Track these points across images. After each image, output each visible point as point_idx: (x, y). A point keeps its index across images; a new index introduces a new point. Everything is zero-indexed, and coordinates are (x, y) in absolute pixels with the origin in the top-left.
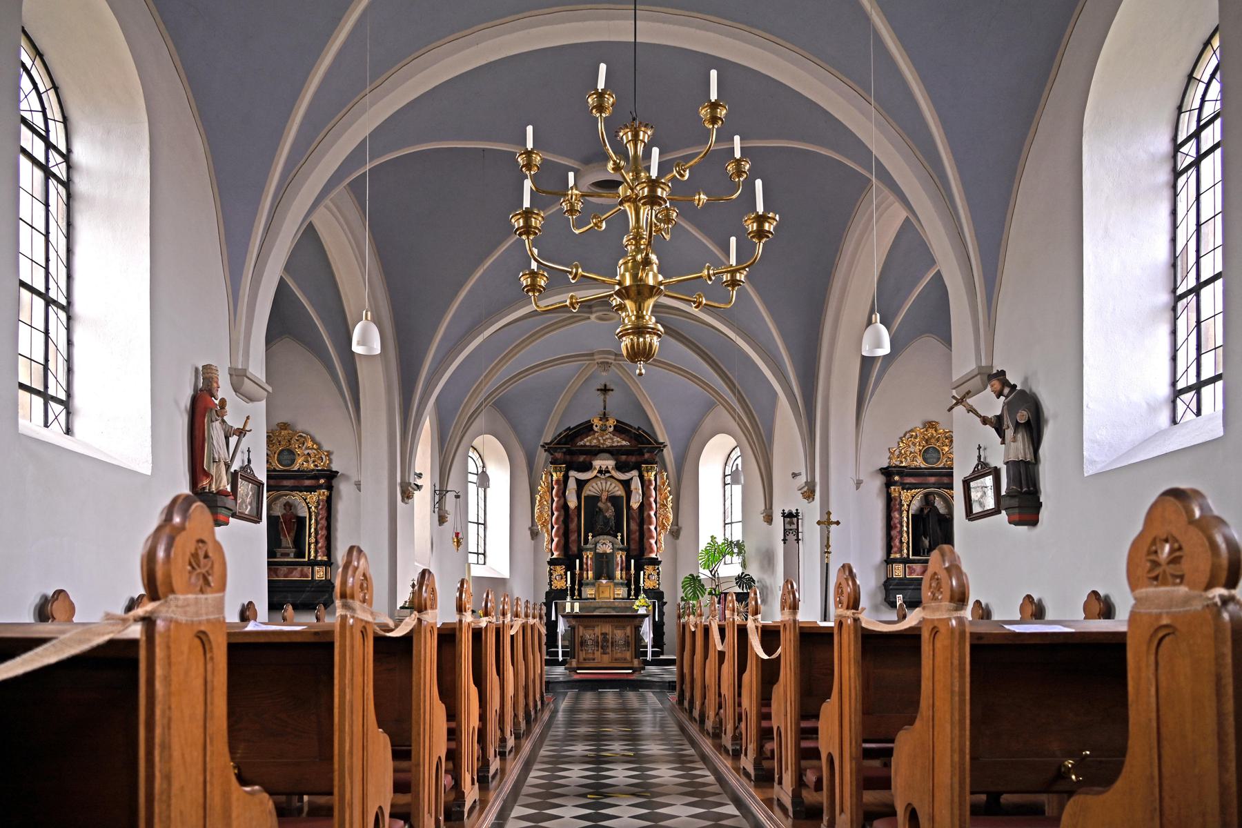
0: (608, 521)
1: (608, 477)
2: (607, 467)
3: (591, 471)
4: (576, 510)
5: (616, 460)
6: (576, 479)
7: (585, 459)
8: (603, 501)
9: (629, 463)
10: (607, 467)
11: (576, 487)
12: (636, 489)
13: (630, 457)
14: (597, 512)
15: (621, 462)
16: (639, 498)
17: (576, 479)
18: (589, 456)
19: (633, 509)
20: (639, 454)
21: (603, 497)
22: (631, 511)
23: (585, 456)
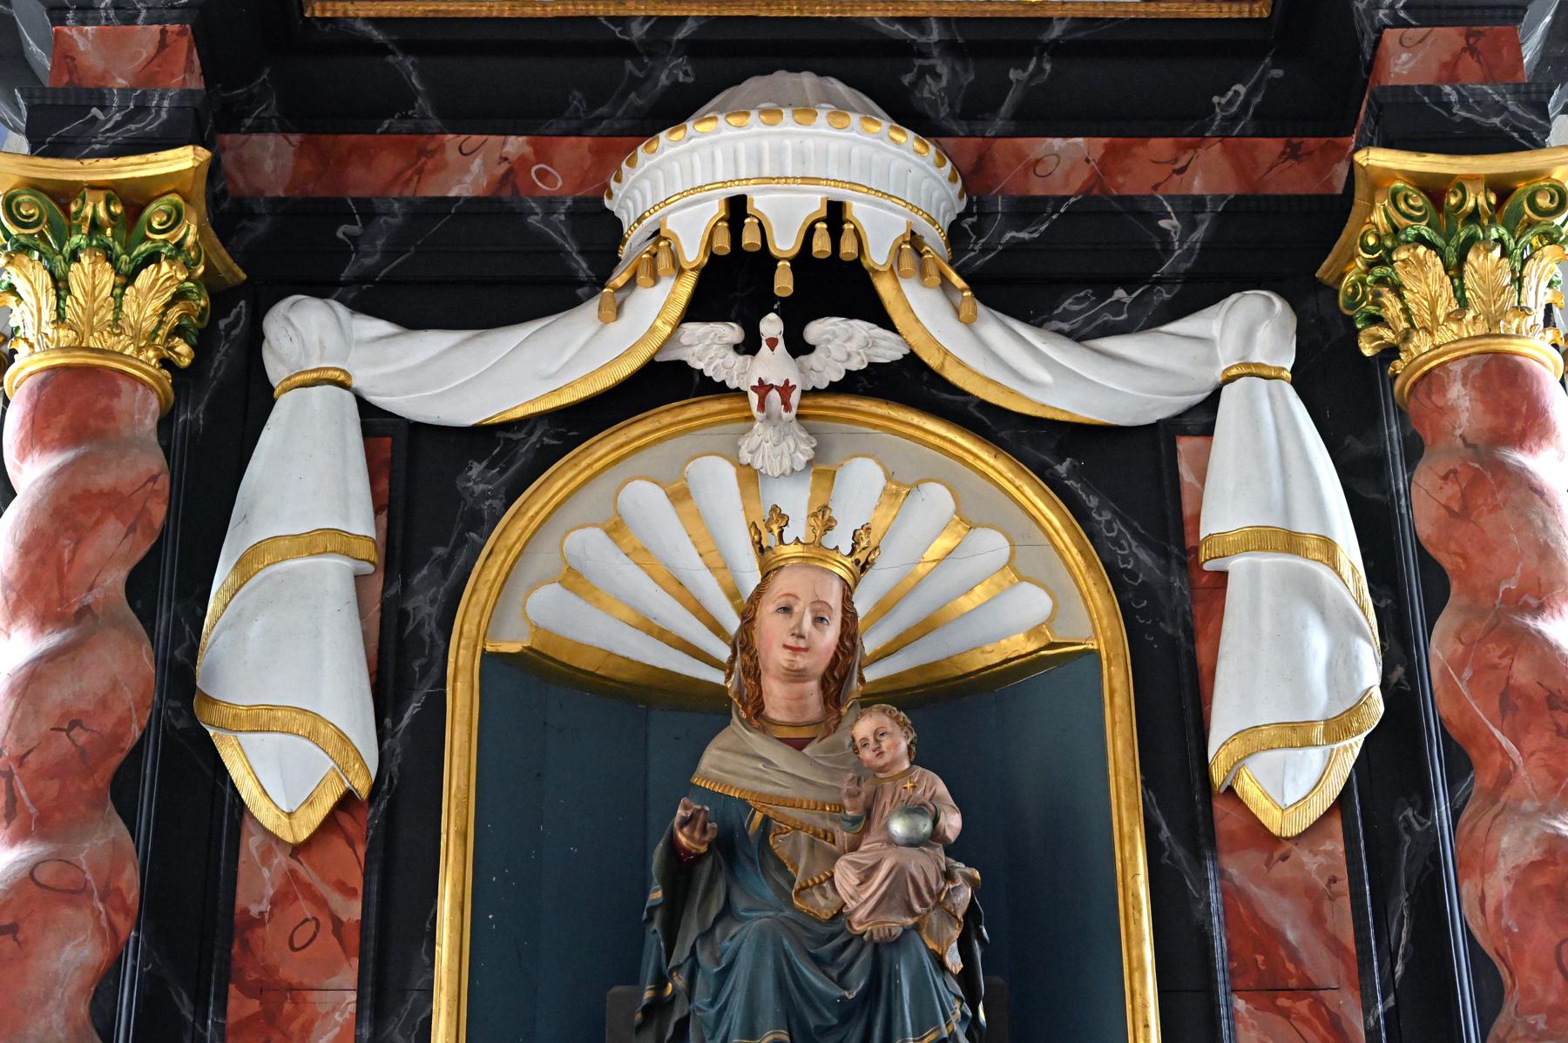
0: (879, 988)
1: (858, 383)
2: (835, 213)
3: (588, 312)
4: (349, 861)
5: (973, 178)
6: (373, 419)
7: (513, 173)
8: (777, 697)
9: (1141, 211)
10: (835, 213)
11: (361, 521)
12: (1290, 542)
13: (1161, 146)
14: (681, 867)
15: (1026, 209)
16: (1341, 663)
17: (373, 419)
18: (573, 150)
19: (1260, 835)
20: (1269, 121)
21: (773, 631)
22: (1237, 866)
23: (515, 145)
